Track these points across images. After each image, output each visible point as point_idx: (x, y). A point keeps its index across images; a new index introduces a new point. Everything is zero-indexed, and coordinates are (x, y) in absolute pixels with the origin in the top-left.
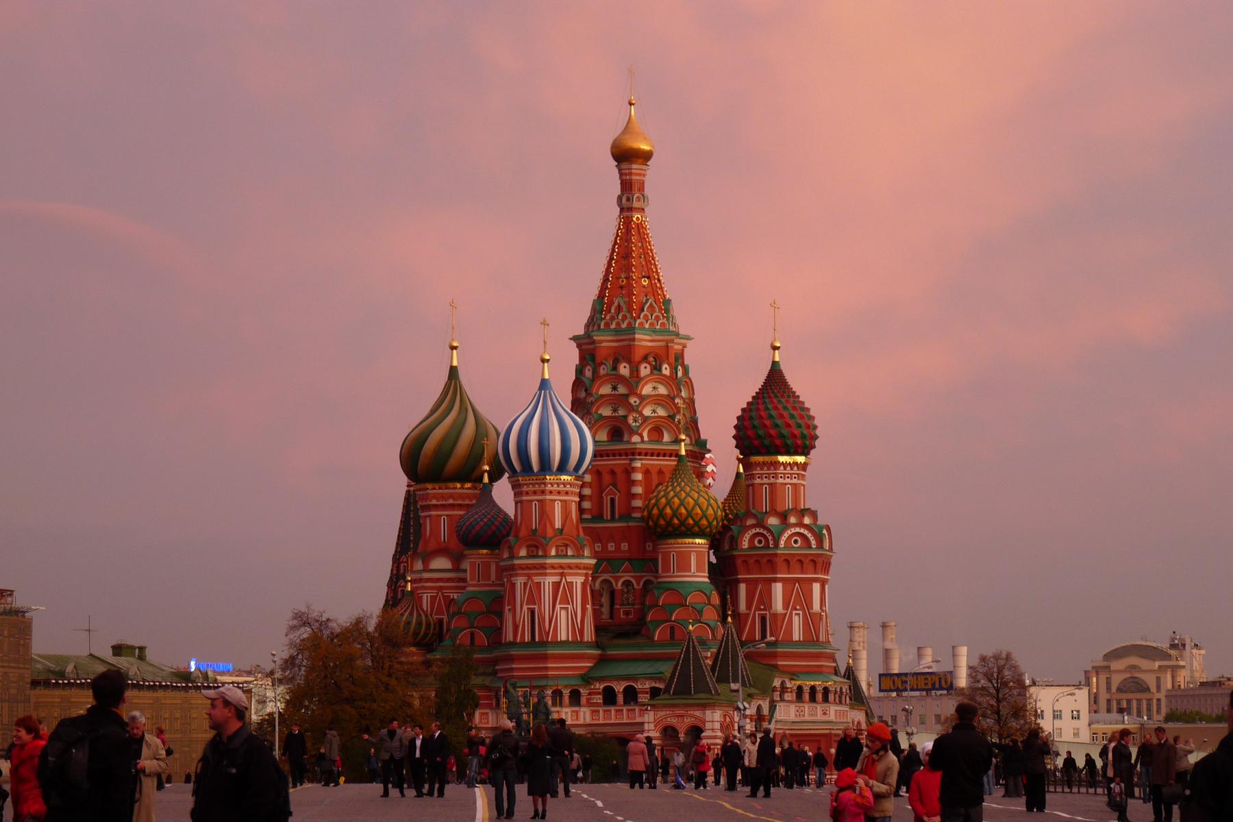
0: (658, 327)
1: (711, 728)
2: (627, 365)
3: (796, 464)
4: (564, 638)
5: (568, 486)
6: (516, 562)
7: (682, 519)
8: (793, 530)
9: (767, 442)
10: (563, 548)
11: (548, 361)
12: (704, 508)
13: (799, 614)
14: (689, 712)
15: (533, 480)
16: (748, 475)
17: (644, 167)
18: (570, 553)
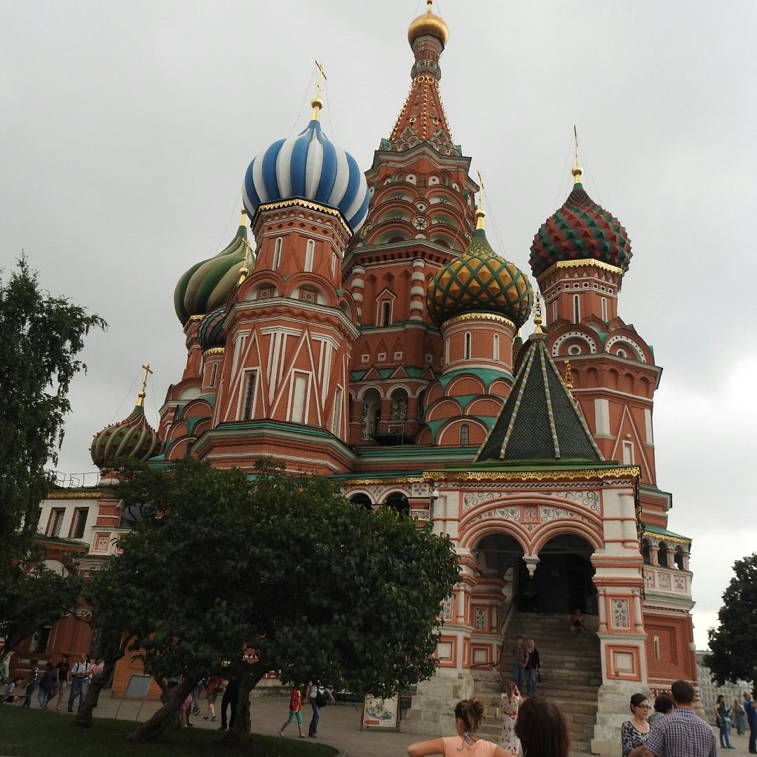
0: (448, 154)
1: (619, 537)
2: (414, 176)
3: (614, 275)
4: (297, 418)
5: (329, 223)
6: (239, 307)
7: (485, 282)
8: (619, 339)
9: (579, 242)
10: (309, 293)
11: (320, 106)
12: (515, 274)
13: (630, 444)
14: (554, 495)
15: (279, 207)
16: (546, 293)
17: (440, 44)
18: (320, 301)
